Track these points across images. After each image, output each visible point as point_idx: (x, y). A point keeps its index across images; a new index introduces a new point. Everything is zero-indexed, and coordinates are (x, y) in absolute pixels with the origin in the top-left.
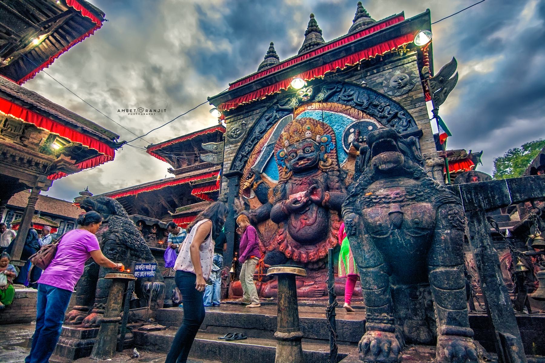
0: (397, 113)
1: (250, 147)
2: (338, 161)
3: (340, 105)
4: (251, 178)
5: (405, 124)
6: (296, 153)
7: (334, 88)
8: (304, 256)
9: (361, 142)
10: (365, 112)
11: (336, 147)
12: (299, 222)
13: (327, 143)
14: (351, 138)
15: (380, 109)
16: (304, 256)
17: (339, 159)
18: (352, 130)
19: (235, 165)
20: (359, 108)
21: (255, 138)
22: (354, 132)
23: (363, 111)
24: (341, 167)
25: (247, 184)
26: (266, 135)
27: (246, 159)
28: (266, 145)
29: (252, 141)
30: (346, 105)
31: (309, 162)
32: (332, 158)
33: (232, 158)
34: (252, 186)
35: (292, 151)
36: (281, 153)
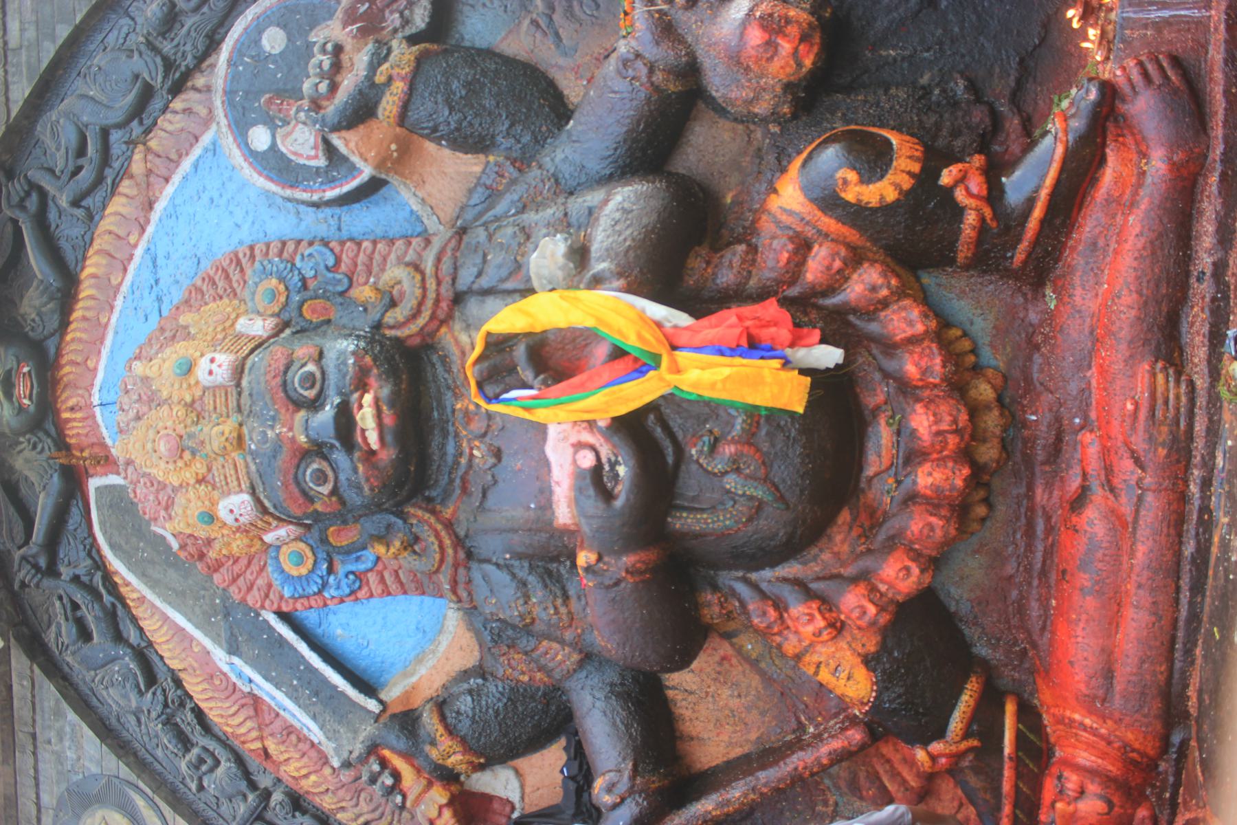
1: (217, 763)
3: (117, 205)
4: (396, 775)
7: (15, 222)
8: (926, 478)
9: (334, 87)
10: (187, 75)
11: (326, 243)
12: (731, 482)
18: (260, 138)
20: (157, 104)
21: (169, 722)
22: (270, 123)
23: (177, 89)
26: (171, 655)
27: (277, 797)
28: (220, 656)
29: (185, 743)
30: (124, 173)
31: (373, 381)
34: (448, 777)
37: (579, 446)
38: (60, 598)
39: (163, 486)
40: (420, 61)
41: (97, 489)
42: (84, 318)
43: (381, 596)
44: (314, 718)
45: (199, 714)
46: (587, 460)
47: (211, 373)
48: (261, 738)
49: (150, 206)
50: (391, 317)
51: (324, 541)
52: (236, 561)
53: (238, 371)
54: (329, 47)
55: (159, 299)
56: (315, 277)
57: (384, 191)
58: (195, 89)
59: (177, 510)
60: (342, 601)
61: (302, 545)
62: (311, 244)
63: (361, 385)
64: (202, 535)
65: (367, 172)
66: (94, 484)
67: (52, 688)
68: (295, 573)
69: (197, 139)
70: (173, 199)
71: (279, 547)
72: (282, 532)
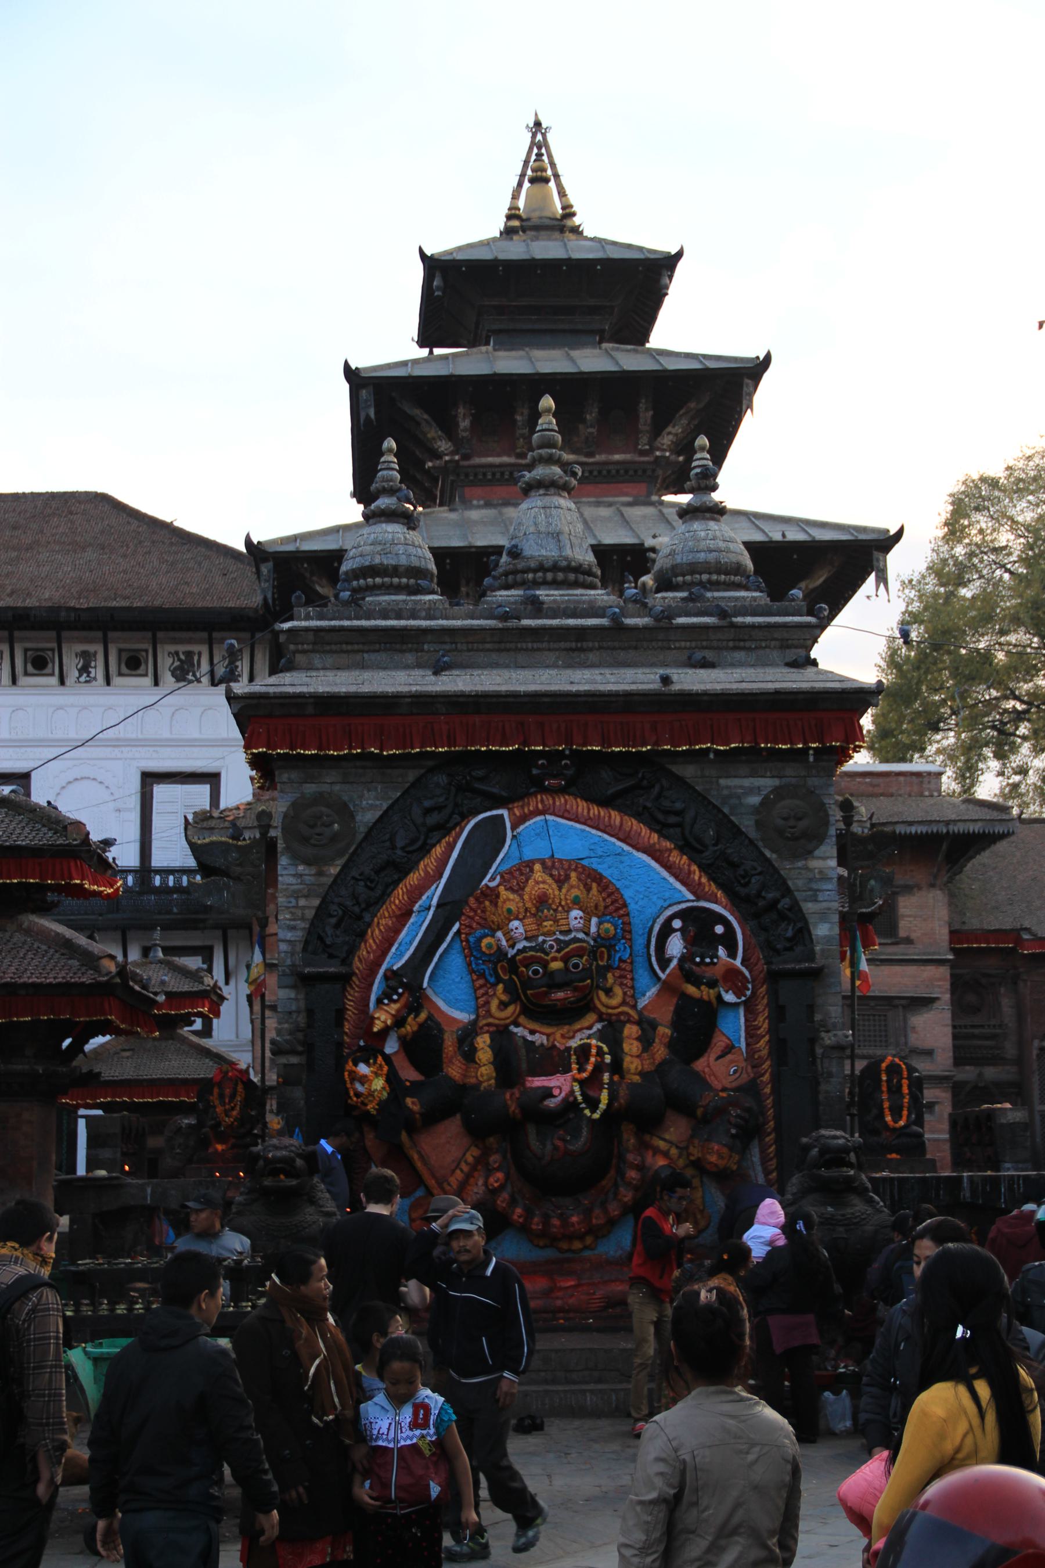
0: (776, 902)
2: (633, 996)
3: (645, 831)
4: (395, 1001)
5: (790, 933)
6: (545, 964)
8: (556, 1222)
10: (706, 873)
11: (631, 955)
13: (613, 942)
14: (676, 946)
15: (744, 877)
16: (556, 1222)
17: (637, 985)
18: (677, 924)
19: (320, 938)
21: (391, 864)
24: (640, 1006)
25: (382, 1018)
29: (377, 872)
32: (621, 984)
33: (310, 914)
35: (533, 960)
36: (485, 941)
37: (561, 1089)
38: (447, 799)
39: (523, 889)
40: (709, 1002)
41: (502, 816)
42: (589, 810)
43: (474, 986)
44: (414, 954)
45: (396, 883)
46: (556, 1092)
47: (576, 918)
48: (390, 917)
49: (645, 852)
50: (602, 994)
51: (500, 961)
52: (483, 911)
53: (577, 930)
54: (715, 960)
55: (601, 857)
56: (616, 951)
57: (655, 979)
58: (700, 878)
59: (511, 896)
60: (469, 964)
61: (495, 948)
62: (631, 947)
63: (576, 989)
64: (500, 904)
65: (663, 976)
66: (504, 812)
67: (399, 794)
68: (483, 945)
69: (677, 877)
70: (649, 866)
71: (493, 936)
72: (504, 943)
